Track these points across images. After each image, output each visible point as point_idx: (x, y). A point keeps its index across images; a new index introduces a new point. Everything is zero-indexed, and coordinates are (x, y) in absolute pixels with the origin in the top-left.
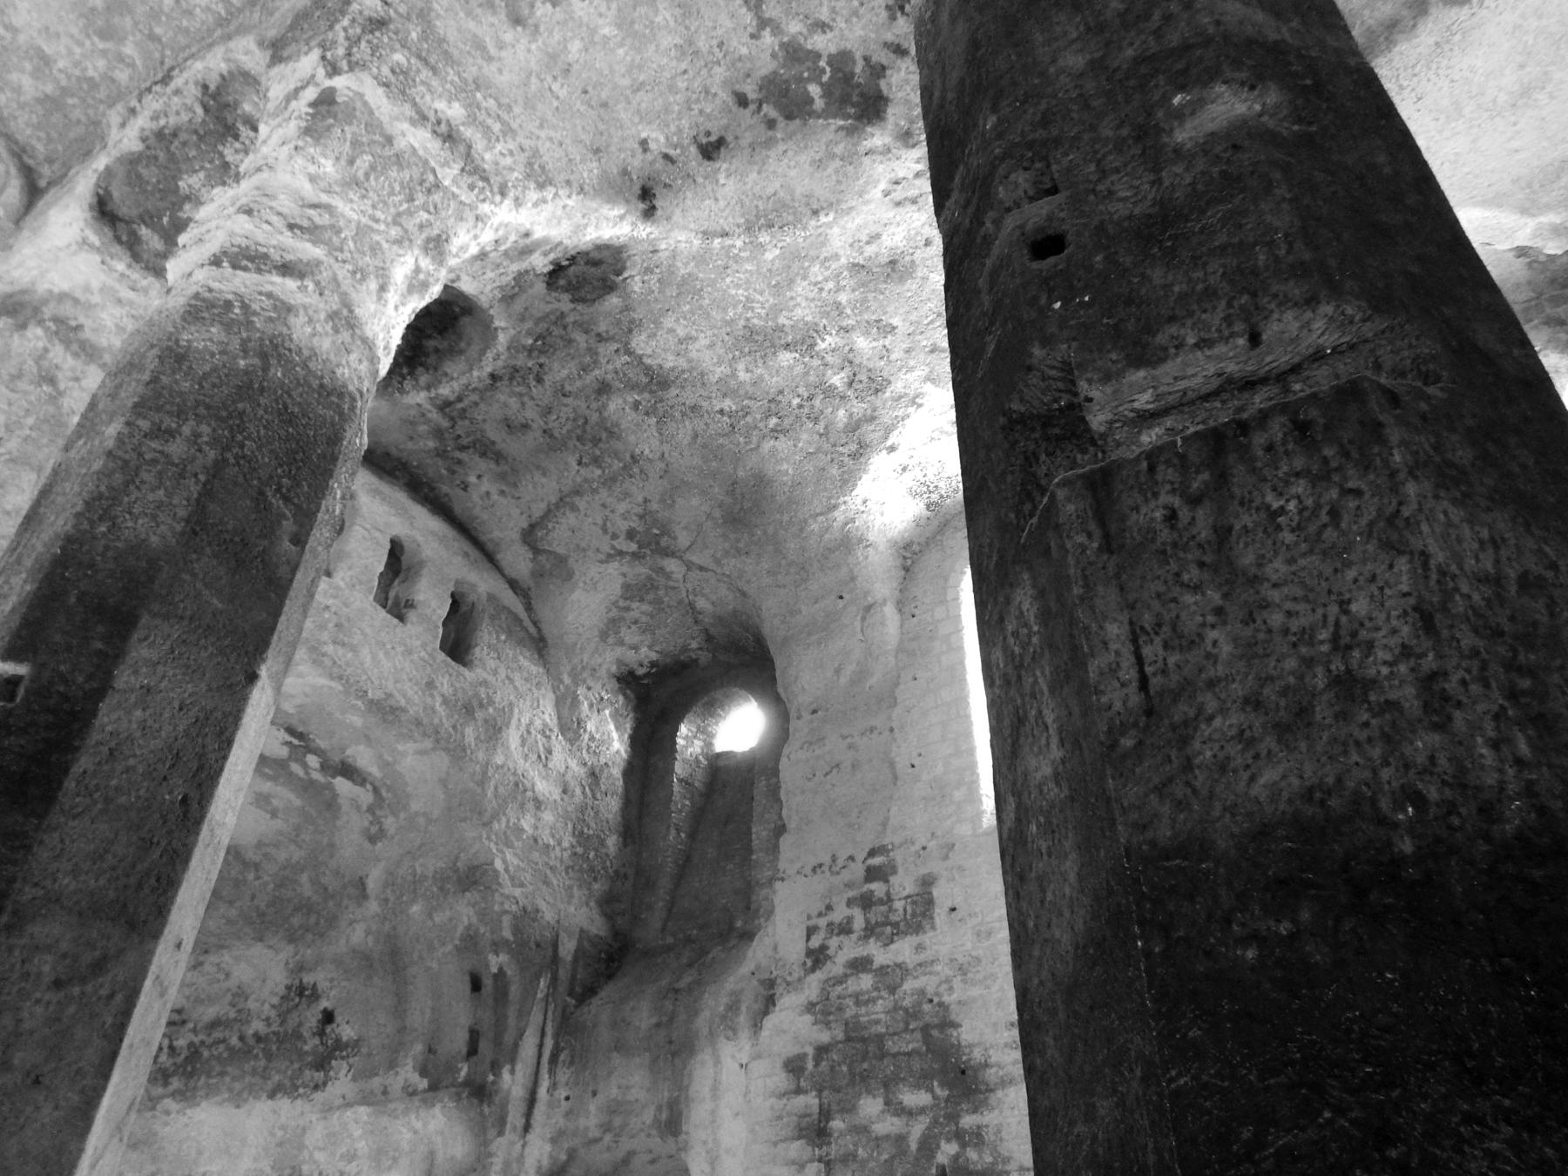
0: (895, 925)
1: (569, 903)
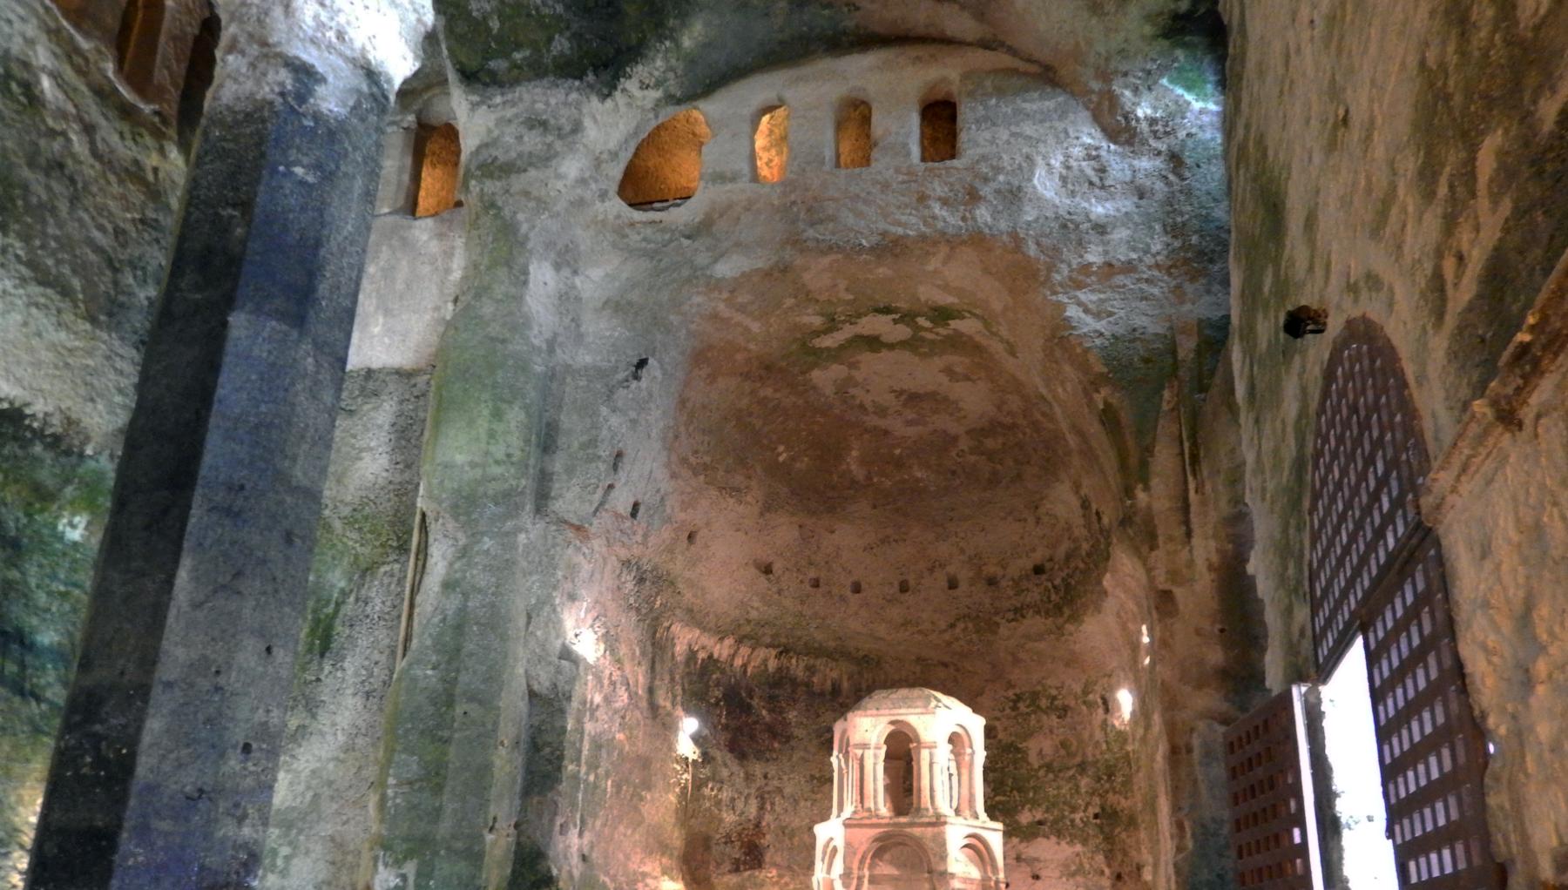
1: (1182, 303)
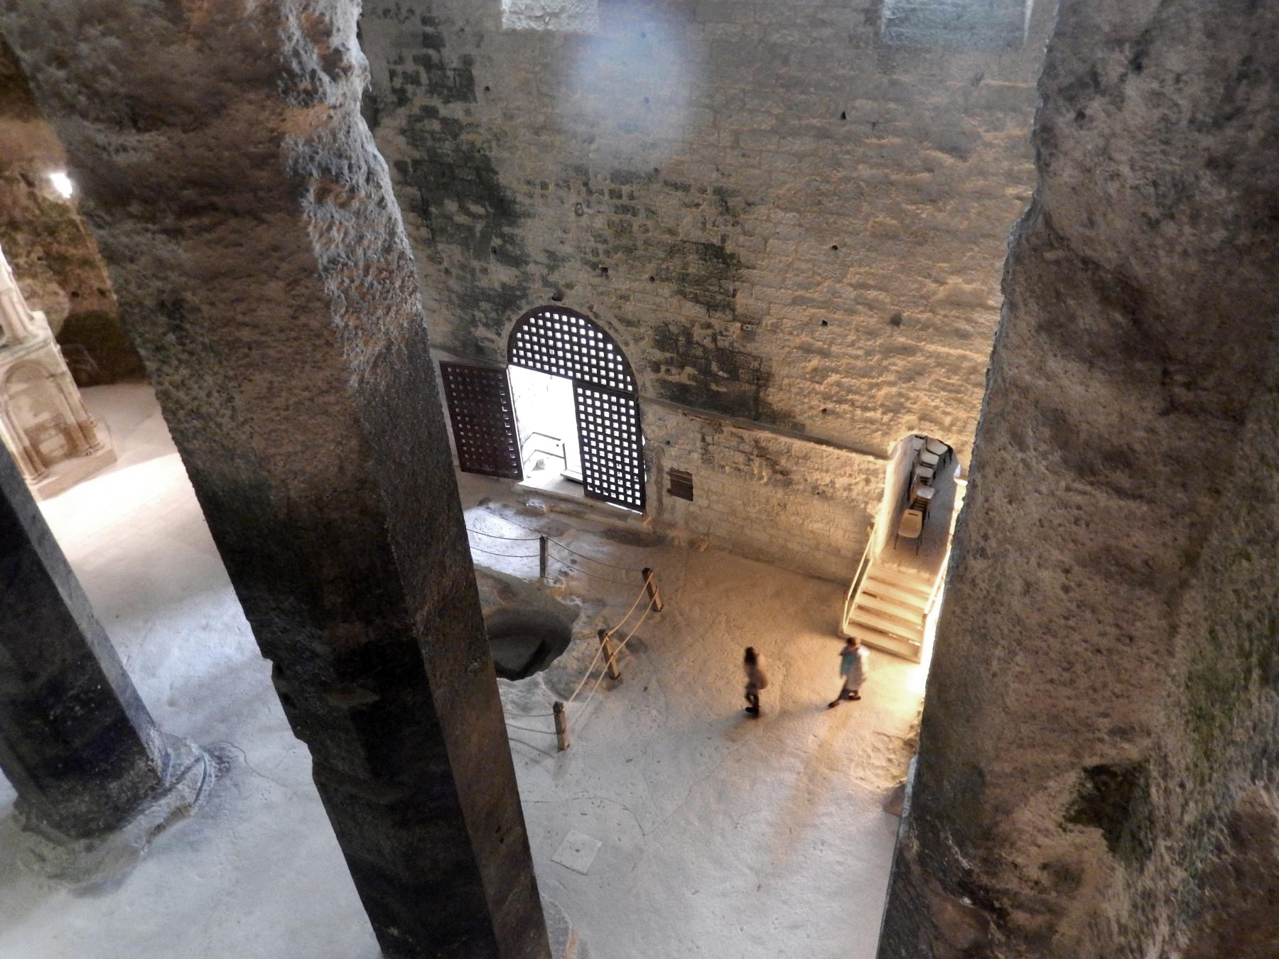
0: (450, 89)
